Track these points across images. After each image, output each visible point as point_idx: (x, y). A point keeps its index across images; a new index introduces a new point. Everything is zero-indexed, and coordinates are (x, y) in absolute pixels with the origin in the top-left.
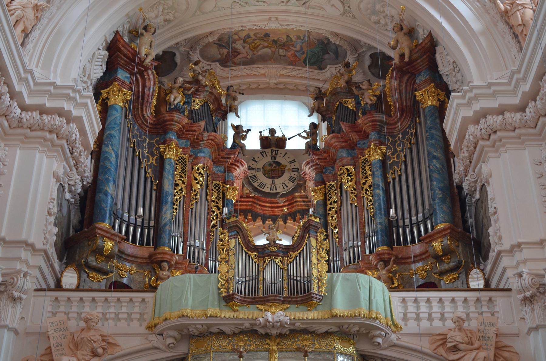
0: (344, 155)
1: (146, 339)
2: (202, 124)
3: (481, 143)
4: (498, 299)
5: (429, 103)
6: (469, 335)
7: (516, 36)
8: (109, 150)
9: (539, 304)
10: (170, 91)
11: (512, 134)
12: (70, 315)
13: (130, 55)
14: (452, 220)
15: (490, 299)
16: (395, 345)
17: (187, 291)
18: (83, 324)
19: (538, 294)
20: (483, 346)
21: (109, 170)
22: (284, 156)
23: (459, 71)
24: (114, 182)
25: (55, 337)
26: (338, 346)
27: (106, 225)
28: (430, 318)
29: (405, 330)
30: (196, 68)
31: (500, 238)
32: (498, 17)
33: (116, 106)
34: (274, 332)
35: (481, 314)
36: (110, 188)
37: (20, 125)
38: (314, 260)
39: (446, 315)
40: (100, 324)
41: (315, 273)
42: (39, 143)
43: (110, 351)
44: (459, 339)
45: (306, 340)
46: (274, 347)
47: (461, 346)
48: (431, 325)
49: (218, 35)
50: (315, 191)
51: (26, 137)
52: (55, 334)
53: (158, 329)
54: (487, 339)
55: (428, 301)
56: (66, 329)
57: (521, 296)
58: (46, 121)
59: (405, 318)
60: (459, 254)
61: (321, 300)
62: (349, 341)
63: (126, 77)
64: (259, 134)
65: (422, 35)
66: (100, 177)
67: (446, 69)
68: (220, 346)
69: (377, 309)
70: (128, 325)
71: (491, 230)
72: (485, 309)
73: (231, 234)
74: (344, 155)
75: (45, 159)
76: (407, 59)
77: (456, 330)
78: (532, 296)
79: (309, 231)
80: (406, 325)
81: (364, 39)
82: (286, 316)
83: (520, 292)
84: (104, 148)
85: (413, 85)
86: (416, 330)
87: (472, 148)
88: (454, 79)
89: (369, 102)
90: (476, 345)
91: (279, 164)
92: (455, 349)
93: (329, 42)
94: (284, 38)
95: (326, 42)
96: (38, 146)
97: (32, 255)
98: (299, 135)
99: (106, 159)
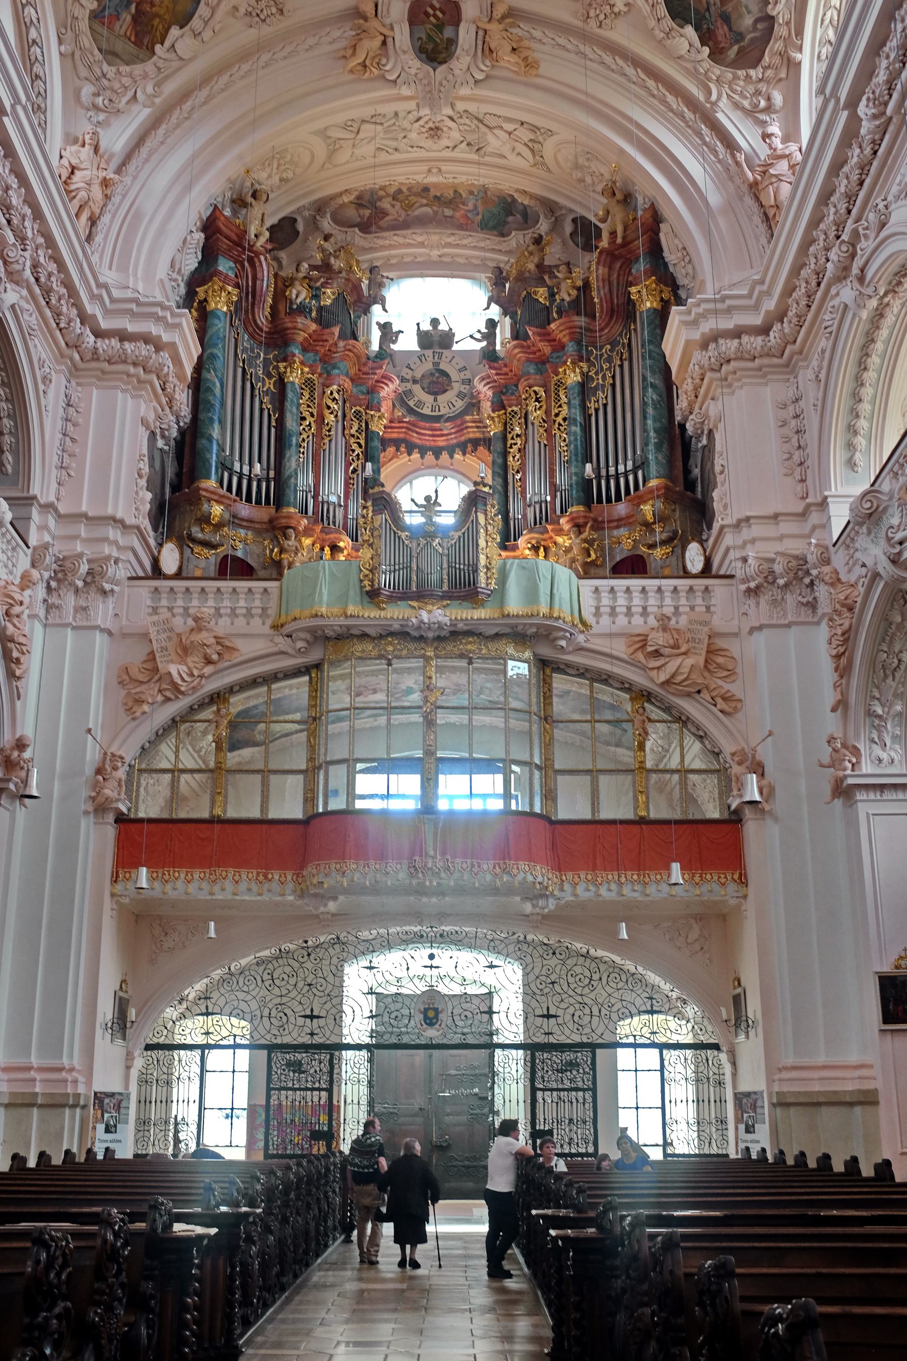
0: (532, 371)
2: (336, 330)
3: (709, 375)
5: (648, 305)
6: (676, 636)
7: (766, 218)
8: (210, 376)
10: (288, 283)
11: (749, 364)
12: (175, 611)
13: (235, 238)
15: (707, 589)
16: (582, 649)
18: (191, 622)
21: (212, 405)
23: (690, 262)
24: (220, 422)
25: (158, 640)
27: (211, 483)
28: (629, 613)
30: (327, 245)
31: (725, 507)
32: (745, 188)
33: (219, 313)
35: (692, 608)
36: (216, 433)
38: (482, 543)
39: (649, 609)
40: (213, 623)
41: (483, 560)
43: (226, 656)
46: (430, 653)
47: (667, 651)
48: (629, 623)
49: (357, 193)
50: (492, 419)
53: (287, 629)
55: (628, 590)
56: (171, 630)
57: (743, 587)
59: (597, 613)
61: (489, 595)
62: (525, 644)
65: (641, 202)
66: (202, 416)
70: (248, 624)
71: (716, 494)
72: (699, 601)
74: (532, 371)
76: (619, 240)
80: (598, 623)
81: (561, 201)
84: (205, 374)
87: (698, 381)
88: (683, 271)
89: (567, 298)
90: (683, 650)
92: (657, 654)
93: (514, 200)
94: (450, 194)
95: (509, 200)
97: (122, 533)
98: (471, 336)
99: (209, 390)
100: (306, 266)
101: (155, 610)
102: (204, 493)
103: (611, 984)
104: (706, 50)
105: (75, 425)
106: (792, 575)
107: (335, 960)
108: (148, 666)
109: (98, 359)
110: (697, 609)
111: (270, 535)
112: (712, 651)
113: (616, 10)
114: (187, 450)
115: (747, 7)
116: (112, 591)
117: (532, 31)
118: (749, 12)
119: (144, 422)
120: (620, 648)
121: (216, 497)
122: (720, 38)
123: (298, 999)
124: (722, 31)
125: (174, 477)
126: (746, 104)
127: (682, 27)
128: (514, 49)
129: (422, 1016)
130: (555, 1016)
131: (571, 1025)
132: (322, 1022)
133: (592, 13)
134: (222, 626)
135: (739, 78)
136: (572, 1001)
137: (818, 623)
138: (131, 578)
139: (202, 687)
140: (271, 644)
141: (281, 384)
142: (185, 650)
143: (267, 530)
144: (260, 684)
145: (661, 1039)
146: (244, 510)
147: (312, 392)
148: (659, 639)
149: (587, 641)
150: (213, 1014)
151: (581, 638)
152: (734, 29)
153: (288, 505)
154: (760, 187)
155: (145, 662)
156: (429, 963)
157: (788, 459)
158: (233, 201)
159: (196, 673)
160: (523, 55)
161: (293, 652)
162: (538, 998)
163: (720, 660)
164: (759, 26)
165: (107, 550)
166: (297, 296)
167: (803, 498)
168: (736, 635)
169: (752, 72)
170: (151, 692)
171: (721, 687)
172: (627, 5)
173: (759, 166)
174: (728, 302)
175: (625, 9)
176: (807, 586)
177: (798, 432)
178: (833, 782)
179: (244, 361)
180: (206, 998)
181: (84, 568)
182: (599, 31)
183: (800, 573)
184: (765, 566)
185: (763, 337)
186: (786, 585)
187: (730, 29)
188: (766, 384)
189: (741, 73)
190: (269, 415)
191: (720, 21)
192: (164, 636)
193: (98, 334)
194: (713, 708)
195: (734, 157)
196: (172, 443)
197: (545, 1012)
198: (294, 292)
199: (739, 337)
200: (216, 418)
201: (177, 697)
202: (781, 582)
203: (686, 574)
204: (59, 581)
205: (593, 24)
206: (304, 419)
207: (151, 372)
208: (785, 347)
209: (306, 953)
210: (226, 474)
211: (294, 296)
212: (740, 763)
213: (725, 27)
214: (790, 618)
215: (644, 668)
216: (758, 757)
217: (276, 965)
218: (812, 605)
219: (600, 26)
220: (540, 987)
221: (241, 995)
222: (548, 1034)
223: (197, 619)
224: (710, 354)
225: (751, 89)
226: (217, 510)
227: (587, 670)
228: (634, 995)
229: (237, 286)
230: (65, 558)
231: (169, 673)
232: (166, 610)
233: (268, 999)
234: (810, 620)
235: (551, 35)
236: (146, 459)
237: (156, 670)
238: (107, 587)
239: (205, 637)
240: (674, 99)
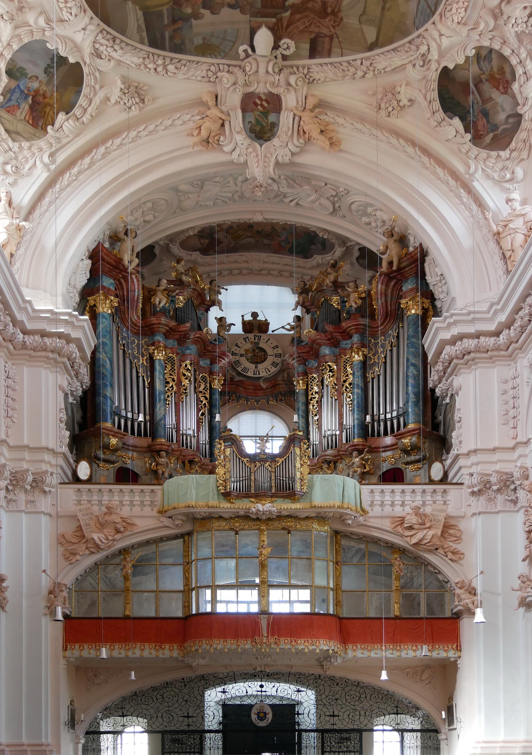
12: (92, 502)
16: (362, 525)
18: (104, 509)
31: (460, 442)
32: (490, 236)
35: (434, 502)
40: (118, 510)
43: (129, 529)
44: (414, 521)
47: (416, 527)
48: (393, 510)
55: (393, 491)
56: (92, 514)
67: (434, 280)
70: (142, 510)
80: (372, 510)
83: (469, 487)
92: (411, 528)
100: (165, 281)
101: (79, 502)
102: (104, 431)
103: (372, 700)
104: (469, 136)
105: (13, 390)
106: (502, 484)
107: (201, 688)
108: (79, 534)
109: (26, 348)
110: (437, 502)
111: (149, 455)
112: (446, 527)
113: (402, 104)
114: (89, 404)
115: (502, 107)
116: (50, 491)
117: (336, 118)
118: (503, 110)
119: (61, 388)
120: (387, 525)
121: (112, 433)
122: (479, 128)
123: (179, 707)
124: (482, 122)
125: (80, 420)
126: (496, 175)
127: (451, 119)
128: (322, 131)
129: (256, 716)
130: (338, 716)
131: (347, 720)
132: (194, 719)
133: (383, 106)
134: (126, 511)
135: (492, 157)
136: (348, 708)
137: (518, 511)
138: (60, 483)
139: (114, 546)
140: (159, 522)
141: (151, 360)
142: (102, 526)
143: (147, 452)
144: (152, 543)
145: (401, 727)
146: (131, 440)
147: (173, 365)
148: (413, 520)
149: (365, 520)
150: (126, 716)
151: (361, 519)
152: (491, 121)
153: (161, 437)
154: (501, 236)
156: (260, 689)
157: (506, 414)
158: (110, 237)
159: (110, 538)
160: (329, 136)
161: (173, 526)
162: (327, 707)
163: (451, 531)
164: (511, 120)
165: (44, 467)
166: (160, 303)
167: (513, 438)
168: (463, 517)
169: (502, 153)
170: (82, 548)
171: (451, 546)
172: (410, 100)
173: (502, 221)
174: (472, 316)
175: (409, 104)
176: (512, 490)
177: (514, 398)
178: (519, 599)
179: (124, 345)
180: (122, 708)
181: (30, 478)
182: (387, 118)
183: (508, 482)
185: (495, 338)
186: (498, 490)
187: (488, 122)
188: (494, 367)
189: (494, 154)
190: (144, 381)
191: (481, 115)
193: (25, 332)
194: (445, 558)
195: (484, 214)
196: (79, 399)
197: (332, 714)
198: (157, 300)
199: (478, 337)
200: (108, 383)
201: (98, 552)
202: (495, 488)
203: (431, 482)
204: (13, 485)
205: (383, 113)
206: (168, 383)
207: (64, 356)
208: (510, 345)
209: (183, 685)
210: (116, 418)
211: (157, 302)
212: (460, 588)
213: (484, 120)
214: (499, 508)
215: (402, 536)
216: (472, 585)
217: (165, 691)
218: (515, 502)
219: (389, 116)
220: (329, 701)
221: (144, 706)
222: (333, 724)
223: (108, 508)
224: (456, 348)
225: (500, 165)
226: (114, 441)
227: (364, 536)
228: (386, 705)
229: (116, 296)
230: (16, 472)
231: (93, 539)
232: (86, 502)
233: (160, 708)
234: (512, 509)
235: (351, 122)
236: (64, 411)
237: (83, 536)
238: (47, 489)
240: (442, 171)
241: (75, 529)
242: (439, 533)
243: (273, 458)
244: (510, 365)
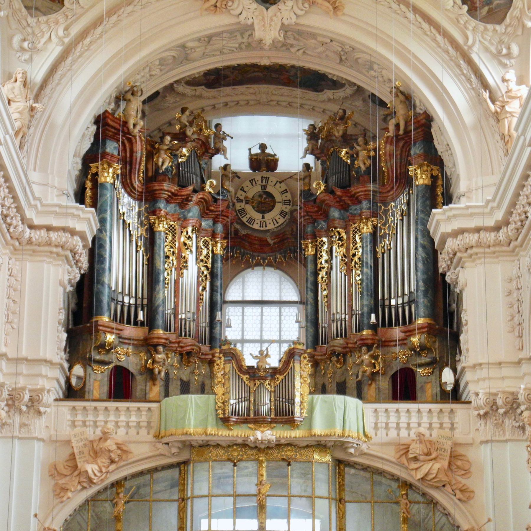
1: (154, 446)
4: (458, 410)
6: (429, 446)
9: (491, 420)
14: (432, 314)
16: (365, 454)
17: (189, 413)
19: (491, 412)
20: (440, 457)
22: (275, 185)
25: (77, 446)
26: (316, 456)
29: (375, 440)
34: (263, 447)
37: (29, 242)
42: (46, 256)
43: (124, 457)
45: (289, 450)
51: (34, 251)
52: (78, 444)
54: (443, 450)
57: (476, 413)
58: (53, 239)
60: (435, 350)
63: (115, 148)
64: (248, 151)
68: (217, 456)
69: (350, 427)
73: (226, 359)
75: (52, 269)
77: (418, 442)
78: (486, 414)
79: (293, 357)
82: (272, 435)
85: (408, 157)
86: (385, 439)
90: (433, 456)
91: (270, 195)
92: (415, 459)
96: (45, 258)
112: (454, 457)
155: (67, 461)
163: (459, 463)
184: (492, 398)
192: (82, 443)
237: (76, 467)
239: (110, 444)
241: (68, 458)
242: (446, 463)
243: (275, 372)
244: (513, 261)
